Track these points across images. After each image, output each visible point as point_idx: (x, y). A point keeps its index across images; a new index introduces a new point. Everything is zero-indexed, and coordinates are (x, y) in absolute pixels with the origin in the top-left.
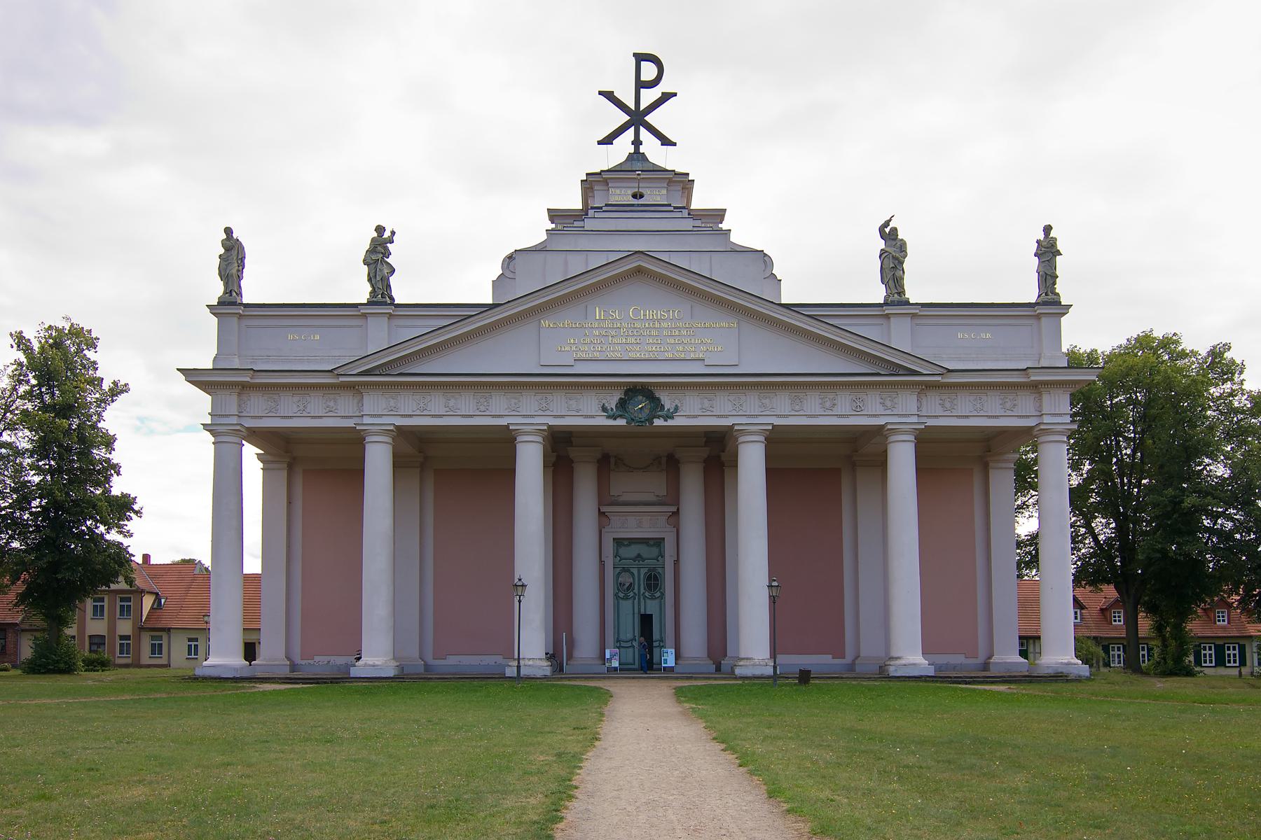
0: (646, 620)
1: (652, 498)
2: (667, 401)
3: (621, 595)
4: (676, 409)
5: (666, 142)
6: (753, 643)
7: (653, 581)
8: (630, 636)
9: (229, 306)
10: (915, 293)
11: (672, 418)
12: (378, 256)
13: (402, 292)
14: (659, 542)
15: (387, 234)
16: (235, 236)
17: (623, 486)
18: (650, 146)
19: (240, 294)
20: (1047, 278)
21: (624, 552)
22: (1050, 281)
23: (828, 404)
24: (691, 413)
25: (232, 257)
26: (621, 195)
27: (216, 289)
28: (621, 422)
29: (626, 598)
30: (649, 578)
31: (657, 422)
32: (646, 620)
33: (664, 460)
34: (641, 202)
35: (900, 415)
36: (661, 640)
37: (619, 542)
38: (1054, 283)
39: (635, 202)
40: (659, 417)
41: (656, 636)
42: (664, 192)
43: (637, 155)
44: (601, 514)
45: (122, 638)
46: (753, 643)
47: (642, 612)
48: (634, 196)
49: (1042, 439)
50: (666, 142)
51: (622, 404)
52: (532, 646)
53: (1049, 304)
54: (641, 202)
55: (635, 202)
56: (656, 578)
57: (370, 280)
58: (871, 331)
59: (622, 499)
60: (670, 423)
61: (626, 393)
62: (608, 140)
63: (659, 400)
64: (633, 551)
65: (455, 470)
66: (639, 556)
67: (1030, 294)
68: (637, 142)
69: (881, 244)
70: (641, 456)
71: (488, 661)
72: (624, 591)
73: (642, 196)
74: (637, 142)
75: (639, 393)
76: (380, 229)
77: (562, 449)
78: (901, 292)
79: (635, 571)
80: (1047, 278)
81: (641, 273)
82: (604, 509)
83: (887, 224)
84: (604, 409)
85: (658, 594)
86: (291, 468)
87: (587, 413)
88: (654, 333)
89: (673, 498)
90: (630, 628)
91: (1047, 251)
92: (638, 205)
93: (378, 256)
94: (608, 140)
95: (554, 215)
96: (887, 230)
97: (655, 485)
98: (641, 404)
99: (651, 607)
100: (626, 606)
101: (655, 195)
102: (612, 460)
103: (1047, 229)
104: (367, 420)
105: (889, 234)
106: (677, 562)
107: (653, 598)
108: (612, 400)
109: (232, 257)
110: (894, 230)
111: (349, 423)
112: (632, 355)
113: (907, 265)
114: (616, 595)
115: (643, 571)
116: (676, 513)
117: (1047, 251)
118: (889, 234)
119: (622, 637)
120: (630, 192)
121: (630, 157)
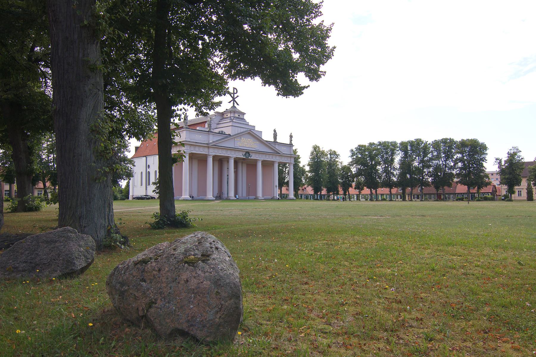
5: (238, 104)
10: (278, 140)
18: (236, 105)
20: (291, 141)
24: (253, 157)
45: (6, 191)
50: (238, 104)
51: (245, 154)
62: (230, 102)
68: (234, 104)
74: (234, 104)
75: (248, 153)
77: (236, 161)
80: (291, 141)
87: (240, 155)
91: (291, 137)
94: (230, 102)
105: (275, 131)
117: (291, 137)
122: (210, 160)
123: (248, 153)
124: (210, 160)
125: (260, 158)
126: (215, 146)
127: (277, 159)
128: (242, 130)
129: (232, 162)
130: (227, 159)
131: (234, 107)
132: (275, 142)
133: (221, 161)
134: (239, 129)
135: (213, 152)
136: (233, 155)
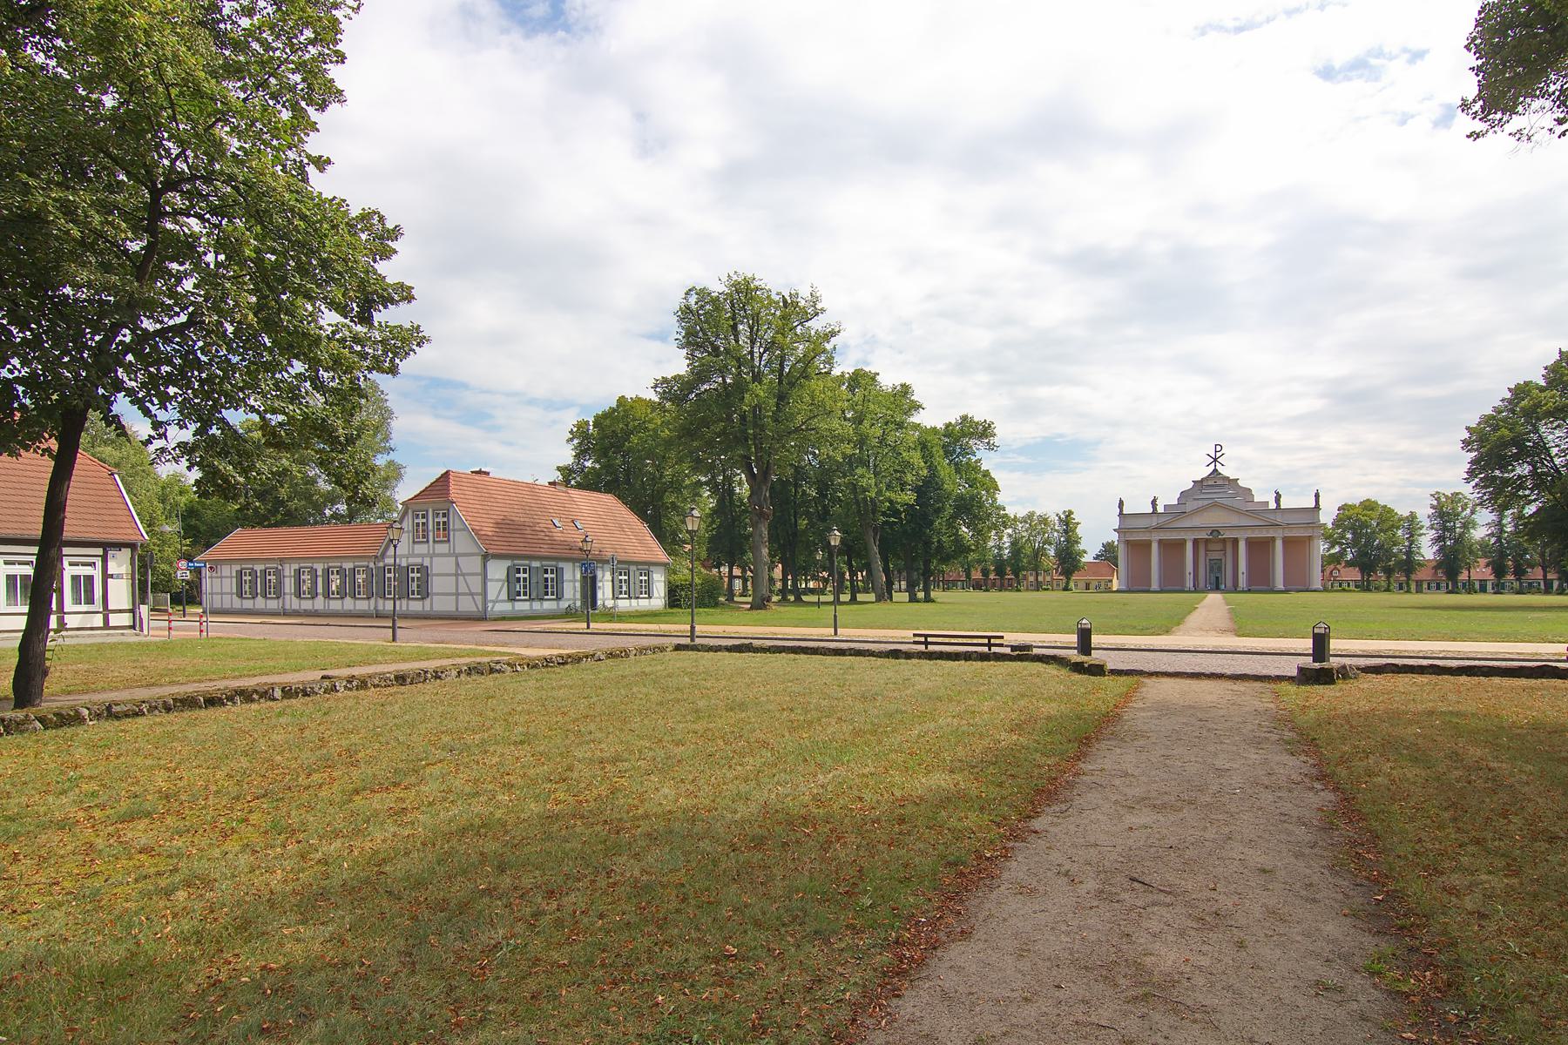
6: (1242, 581)
7: (1220, 569)
12: (1154, 503)
13: (1160, 509)
18: (1219, 467)
25: (1121, 504)
35: (1279, 534)
46: (1242, 581)
52: (1189, 584)
65: (1172, 548)
70: (1215, 544)
72: (1211, 570)
75: (1215, 531)
81: (1215, 505)
87: (1203, 535)
89: (1224, 550)
93: (1154, 503)
97: (1219, 546)
109: (1121, 504)
122: (1155, 547)
124: (1155, 547)
125: (1242, 536)
129: (1189, 546)
130: (1181, 544)
133: (1172, 548)
135: (1155, 537)
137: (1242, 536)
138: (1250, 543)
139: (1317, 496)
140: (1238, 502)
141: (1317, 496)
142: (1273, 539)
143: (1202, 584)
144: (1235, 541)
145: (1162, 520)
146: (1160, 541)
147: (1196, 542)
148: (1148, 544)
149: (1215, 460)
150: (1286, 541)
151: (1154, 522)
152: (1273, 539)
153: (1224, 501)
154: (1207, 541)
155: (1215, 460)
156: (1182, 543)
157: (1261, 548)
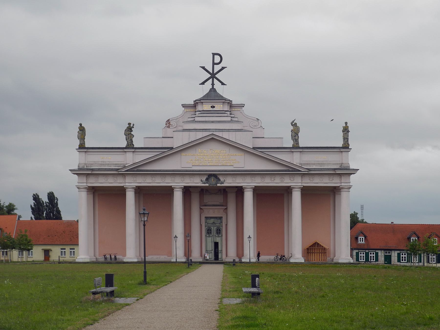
0: (216, 244)
1: (218, 203)
2: (222, 179)
3: (208, 236)
4: (224, 181)
5: (223, 84)
7: (219, 231)
8: (211, 249)
9: (82, 147)
11: (223, 183)
14: (221, 218)
15: (132, 125)
16: (82, 125)
17: (208, 199)
19: (84, 144)
21: (208, 221)
22: (346, 140)
23: (273, 179)
24: (229, 182)
26: (207, 107)
27: (77, 143)
28: (207, 185)
29: (209, 237)
30: (217, 230)
31: (218, 185)
32: (216, 244)
33: (222, 191)
34: (214, 109)
36: (221, 251)
37: (206, 218)
38: (348, 141)
39: (211, 109)
40: (219, 183)
41: (220, 249)
42: (222, 106)
43: (213, 90)
44: (201, 209)
47: (215, 241)
48: (212, 107)
49: (342, 190)
51: (207, 179)
53: (346, 147)
54: (214, 109)
55: (211, 109)
56: (220, 230)
57: (126, 140)
58: (285, 157)
59: (207, 204)
60: (222, 185)
61: (208, 176)
62: (203, 83)
63: (219, 178)
64: (212, 221)
65: (155, 199)
66: (214, 223)
67: (340, 144)
68: (213, 84)
69: (292, 128)
71: (163, 258)
73: (214, 107)
74: (213, 84)
75: (212, 176)
76: (129, 124)
78: (298, 144)
79: (212, 228)
80: (346, 139)
81: (213, 139)
82: (201, 207)
83: (293, 122)
84: (202, 181)
85: (220, 235)
86: (94, 193)
87: (197, 182)
88: (217, 157)
90: (211, 247)
92: (213, 111)
94: (203, 83)
95: (184, 106)
96: (293, 123)
97: (219, 199)
98: (212, 180)
99: (218, 240)
100: (209, 239)
101: (219, 107)
102: (204, 191)
103: (346, 123)
104: (127, 184)
105: (294, 124)
106: (226, 225)
107: (219, 237)
108: (204, 179)
110: (296, 124)
111: (122, 185)
112: (211, 164)
113: (299, 134)
114: (206, 236)
115: (215, 228)
116: (226, 209)
118: (294, 124)
119: (208, 249)
120: (210, 106)
121: (211, 90)
122: (130, 196)
123: (215, 176)
124: (130, 196)
126: (135, 170)
127: (296, 183)
128: (200, 135)
129: (178, 196)
130: (168, 192)
131: (213, 90)
132: (296, 147)
134: (192, 134)
135: (130, 183)
136: (178, 183)
137: (248, 183)
138: (259, 193)
139: (346, 130)
140: (245, 139)
141: (346, 130)
142: (288, 190)
143: (196, 256)
144: (239, 192)
145: (140, 157)
146: (139, 191)
147: (187, 191)
148: (121, 192)
149: (213, 76)
150: (306, 192)
151: (130, 159)
152: (288, 190)
153: (225, 135)
154: (202, 191)
155: (213, 76)
156: (168, 192)
157: (272, 200)
